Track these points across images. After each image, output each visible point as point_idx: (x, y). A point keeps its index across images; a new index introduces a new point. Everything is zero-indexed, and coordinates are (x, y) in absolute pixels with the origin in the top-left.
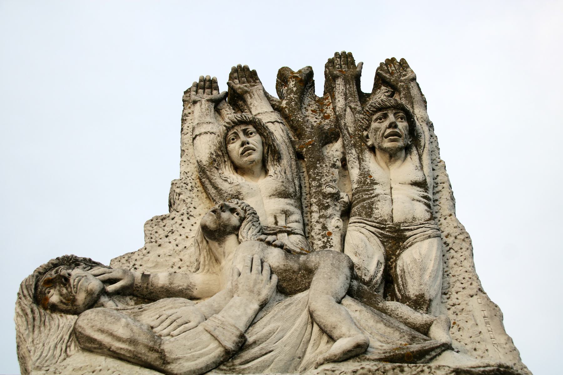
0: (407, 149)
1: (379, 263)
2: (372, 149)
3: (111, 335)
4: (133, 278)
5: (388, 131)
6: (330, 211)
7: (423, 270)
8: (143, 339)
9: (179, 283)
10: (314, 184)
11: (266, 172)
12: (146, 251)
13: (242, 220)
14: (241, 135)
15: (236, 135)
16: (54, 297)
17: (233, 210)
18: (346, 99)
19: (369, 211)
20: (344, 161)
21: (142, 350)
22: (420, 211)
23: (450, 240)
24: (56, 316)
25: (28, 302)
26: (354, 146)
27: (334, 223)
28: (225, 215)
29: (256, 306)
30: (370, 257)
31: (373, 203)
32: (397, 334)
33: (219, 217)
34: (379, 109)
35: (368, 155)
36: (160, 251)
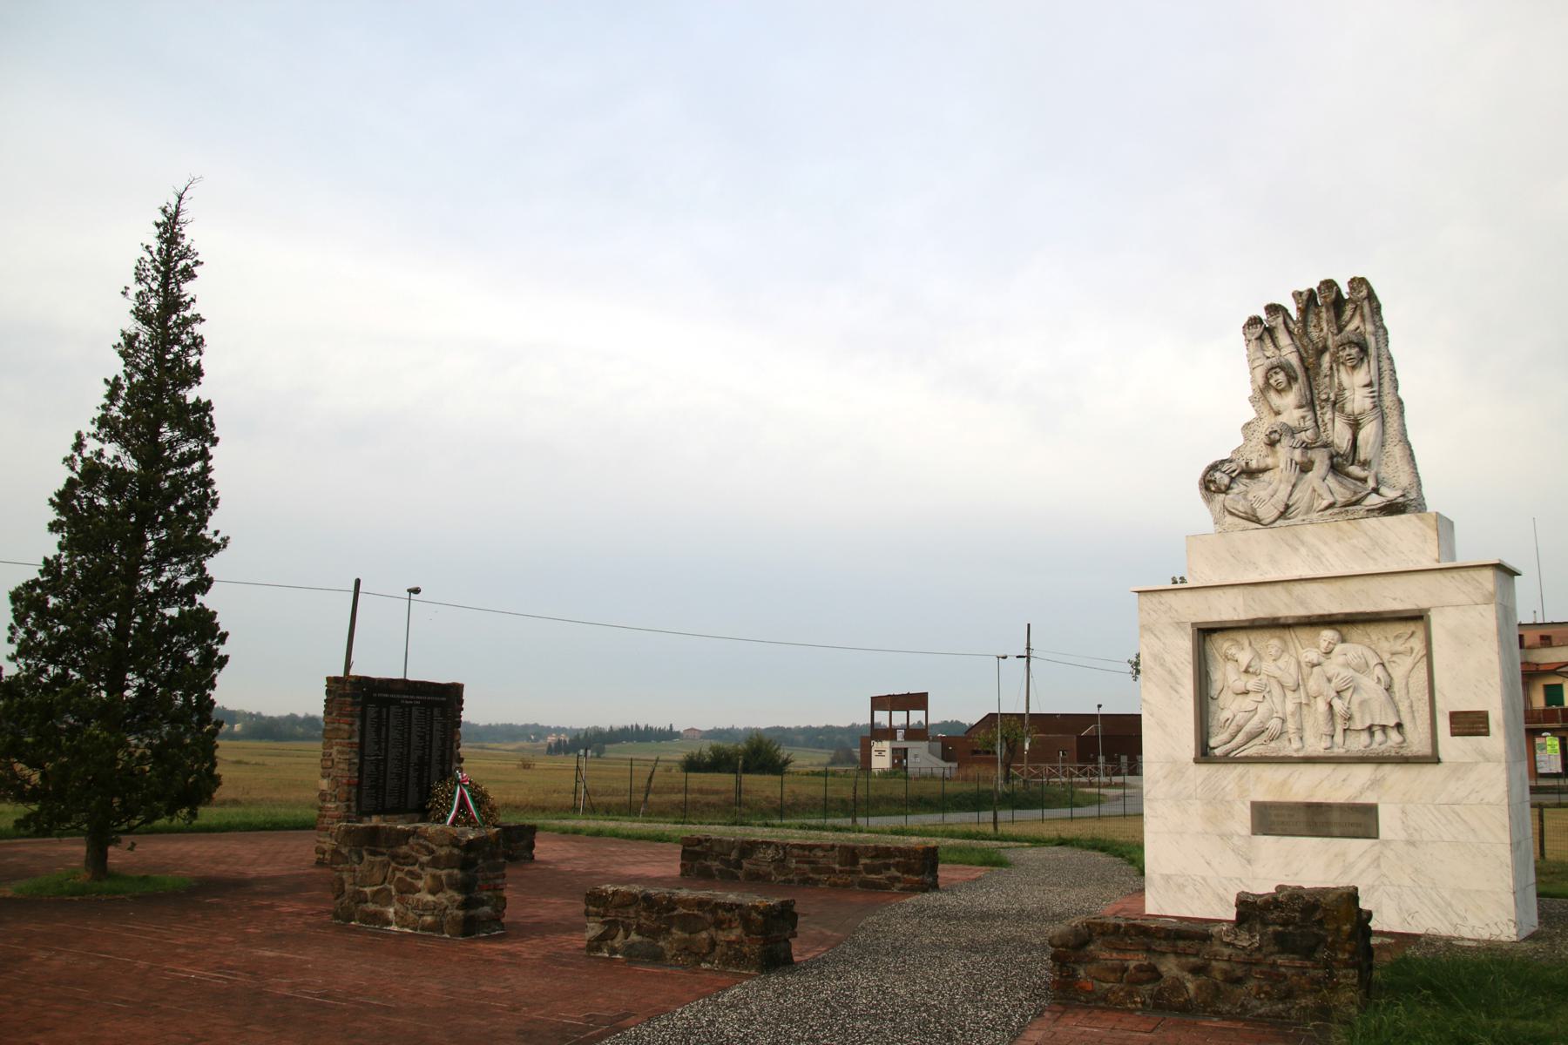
0: (1362, 359)
1: (1349, 440)
2: (1343, 363)
3: (1237, 510)
4: (1242, 467)
5: (1348, 358)
6: (1325, 410)
7: (1367, 443)
8: (1249, 511)
9: (1262, 465)
10: (1317, 391)
11: (1292, 388)
12: (1245, 445)
13: (1281, 435)
14: (1274, 375)
15: (1271, 375)
16: (1213, 489)
17: (1276, 431)
18: (1328, 325)
19: (1342, 410)
20: (1331, 368)
21: (1251, 517)
22: (1368, 403)
23: (1387, 411)
24: (1216, 495)
25: (1204, 491)
26: (1334, 361)
27: (1328, 416)
28: (1272, 436)
29: (1290, 488)
30: (1344, 439)
31: (1344, 404)
32: (1348, 493)
33: (1270, 438)
34: (1340, 346)
35: (1342, 368)
36: (1252, 444)
